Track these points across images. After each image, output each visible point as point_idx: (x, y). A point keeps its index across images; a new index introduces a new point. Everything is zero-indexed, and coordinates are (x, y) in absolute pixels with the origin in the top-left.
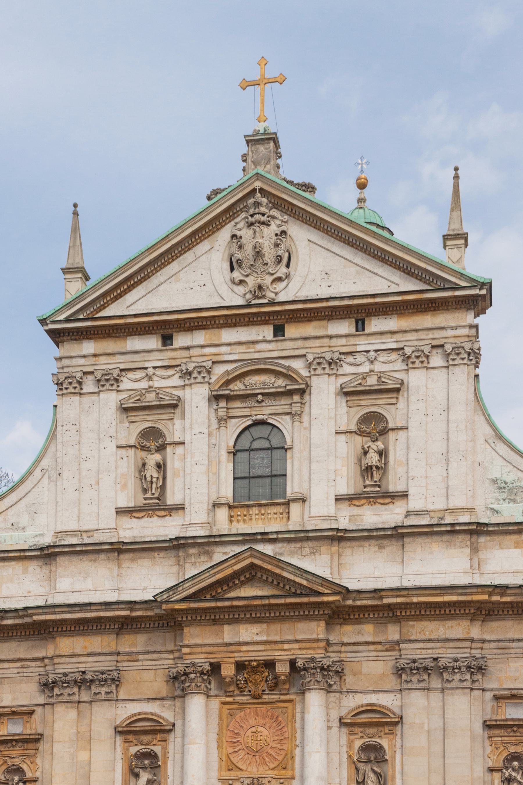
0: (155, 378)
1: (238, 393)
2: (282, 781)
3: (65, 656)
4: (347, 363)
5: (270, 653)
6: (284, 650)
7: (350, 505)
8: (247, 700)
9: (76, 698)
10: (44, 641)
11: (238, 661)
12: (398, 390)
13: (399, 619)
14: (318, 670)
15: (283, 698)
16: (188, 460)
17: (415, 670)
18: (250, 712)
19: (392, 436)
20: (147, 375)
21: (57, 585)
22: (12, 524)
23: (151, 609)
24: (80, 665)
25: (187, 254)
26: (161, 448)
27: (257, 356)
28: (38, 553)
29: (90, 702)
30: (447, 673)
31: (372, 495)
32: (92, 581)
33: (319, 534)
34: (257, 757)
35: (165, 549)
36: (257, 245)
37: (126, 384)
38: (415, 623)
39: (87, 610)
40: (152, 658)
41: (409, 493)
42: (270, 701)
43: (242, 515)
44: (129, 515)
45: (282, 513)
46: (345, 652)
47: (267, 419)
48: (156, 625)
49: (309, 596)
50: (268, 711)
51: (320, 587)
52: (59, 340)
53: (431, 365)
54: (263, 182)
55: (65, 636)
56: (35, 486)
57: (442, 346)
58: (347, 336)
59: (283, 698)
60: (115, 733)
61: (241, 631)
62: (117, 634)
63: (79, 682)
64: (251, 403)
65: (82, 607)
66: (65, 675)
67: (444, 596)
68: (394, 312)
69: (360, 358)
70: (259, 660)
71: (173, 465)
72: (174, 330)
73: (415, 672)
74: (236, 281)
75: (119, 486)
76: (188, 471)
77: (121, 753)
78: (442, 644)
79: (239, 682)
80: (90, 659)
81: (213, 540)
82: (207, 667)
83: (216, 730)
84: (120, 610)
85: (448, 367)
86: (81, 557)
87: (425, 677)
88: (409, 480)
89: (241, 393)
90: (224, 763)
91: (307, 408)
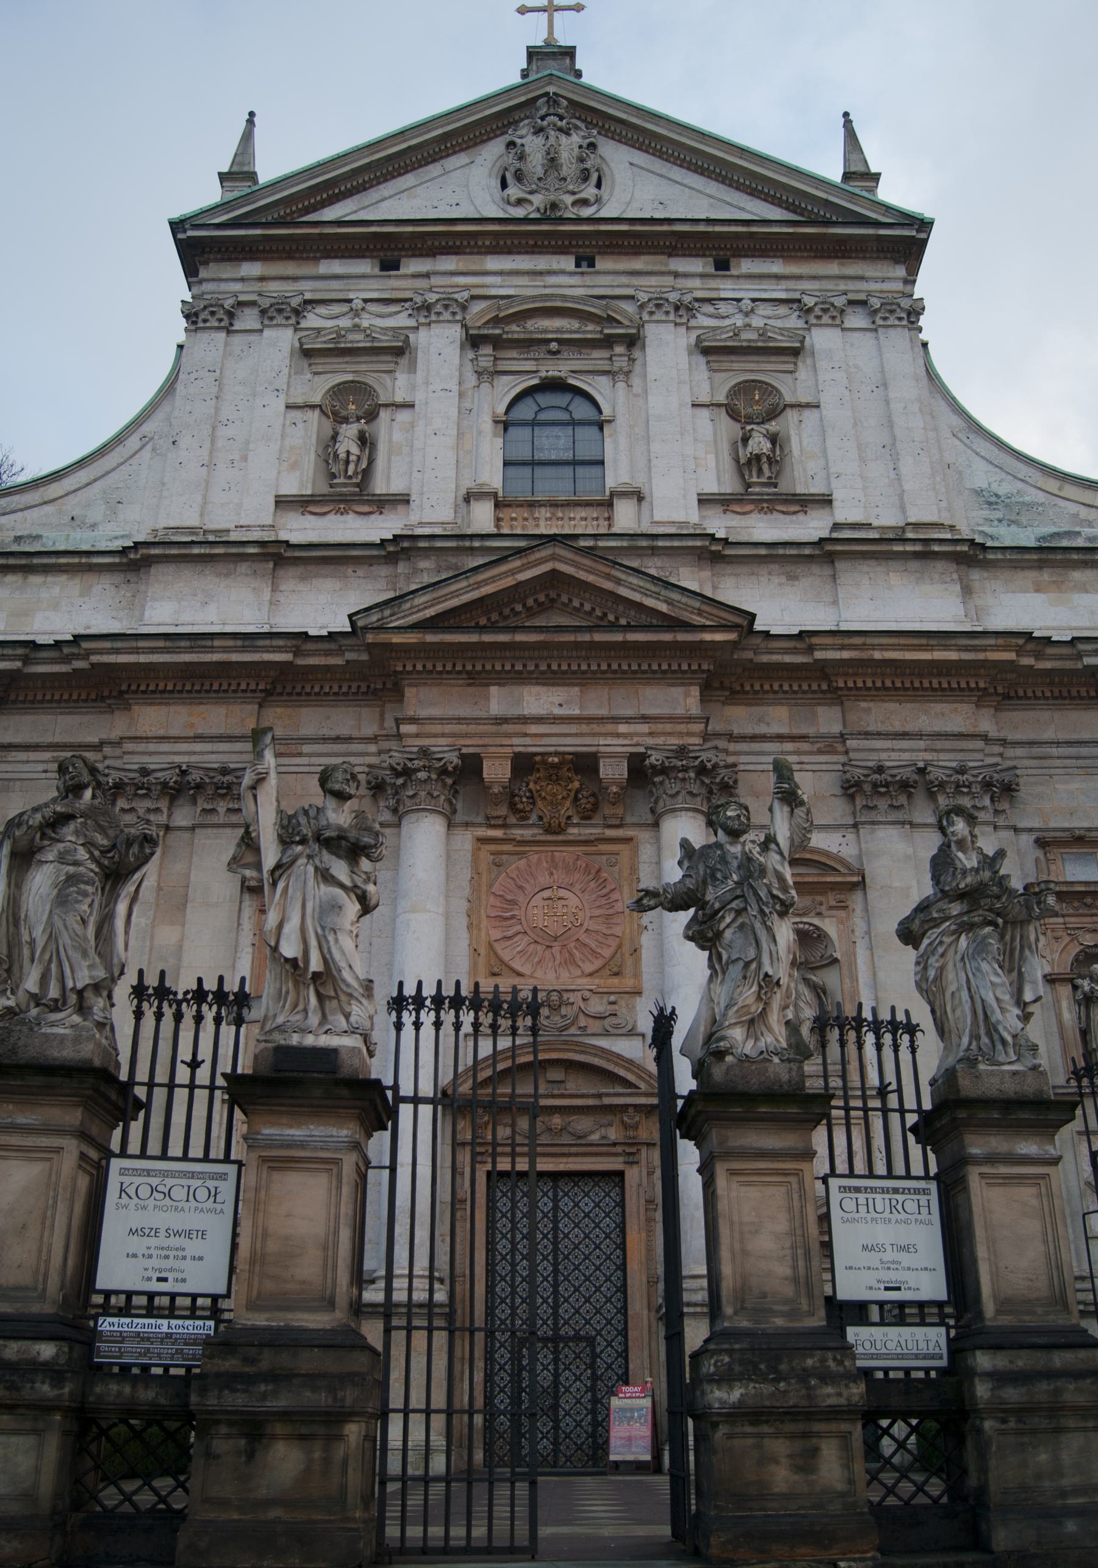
0: (365, 315)
1: (516, 336)
2: (612, 998)
3: (147, 738)
4: (704, 314)
5: (587, 740)
6: (618, 735)
7: (725, 512)
8: (534, 835)
10: (107, 716)
11: (520, 753)
12: (795, 352)
13: (840, 696)
14: (692, 775)
15: (610, 833)
17: (883, 786)
18: (539, 859)
19: (791, 415)
20: (352, 309)
21: (147, 614)
22: (73, 518)
23: (340, 652)
24: (178, 759)
25: (431, 167)
26: (371, 416)
27: (548, 291)
28: (117, 560)
29: (193, 828)
30: (945, 796)
34: (556, 949)
35: (368, 561)
36: (552, 150)
37: (312, 320)
38: (872, 704)
39: (205, 647)
40: (330, 751)
41: (834, 496)
42: (580, 838)
43: (520, 519)
44: (301, 510)
45: (597, 519)
46: (735, 753)
48: (344, 689)
49: (675, 631)
50: (577, 859)
51: (694, 617)
52: (202, 259)
53: (846, 325)
54: (559, 87)
55: (151, 704)
56: (125, 461)
57: (863, 303)
58: (702, 276)
59: (610, 833)
60: (242, 892)
62: (260, 706)
63: (172, 788)
64: (539, 352)
65: (195, 639)
66: (144, 772)
67: (932, 650)
69: (724, 308)
70: (564, 753)
71: (391, 435)
73: (883, 790)
74: (513, 199)
75: (285, 464)
76: (418, 444)
77: (251, 933)
78: (929, 742)
79: (517, 799)
80: (198, 747)
81: (467, 544)
82: (453, 758)
83: (467, 891)
84: (274, 652)
85: (876, 330)
86: (199, 568)
87: (903, 800)
88: (832, 478)
89: (522, 336)
90: (481, 960)
91: (637, 367)
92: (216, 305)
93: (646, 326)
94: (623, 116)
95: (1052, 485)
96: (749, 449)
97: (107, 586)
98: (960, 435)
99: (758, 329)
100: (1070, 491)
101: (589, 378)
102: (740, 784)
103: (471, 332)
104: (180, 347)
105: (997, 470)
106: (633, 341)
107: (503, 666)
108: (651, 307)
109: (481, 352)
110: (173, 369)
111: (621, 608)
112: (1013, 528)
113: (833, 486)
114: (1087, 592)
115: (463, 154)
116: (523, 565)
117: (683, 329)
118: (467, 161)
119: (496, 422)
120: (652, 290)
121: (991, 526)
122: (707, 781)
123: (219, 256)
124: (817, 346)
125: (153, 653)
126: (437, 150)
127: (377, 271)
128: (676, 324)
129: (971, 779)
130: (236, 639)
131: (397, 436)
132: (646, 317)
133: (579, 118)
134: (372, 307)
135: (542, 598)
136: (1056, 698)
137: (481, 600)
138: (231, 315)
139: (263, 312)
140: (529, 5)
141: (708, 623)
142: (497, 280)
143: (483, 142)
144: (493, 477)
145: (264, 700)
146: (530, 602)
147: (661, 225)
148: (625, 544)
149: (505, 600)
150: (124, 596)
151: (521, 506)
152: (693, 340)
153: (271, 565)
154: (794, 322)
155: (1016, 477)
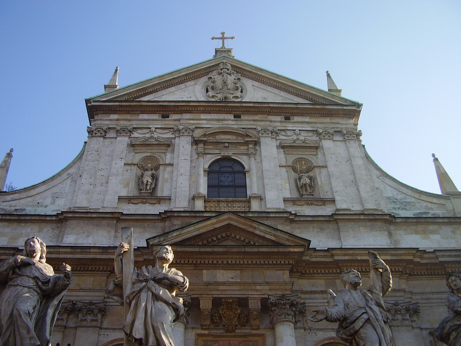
0: (155, 133)
6: (256, 290)
7: (294, 205)
8: (222, 333)
9: (64, 323)
11: (216, 298)
14: (288, 307)
16: (175, 174)
19: (317, 170)
21: (64, 240)
22: (38, 203)
24: (72, 298)
25: (181, 85)
26: (157, 168)
31: (309, 199)
32: (93, 238)
33: (277, 215)
37: (135, 135)
39: (87, 252)
44: (128, 202)
46: (304, 299)
47: (231, 156)
51: (286, 242)
53: (334, 139)
57: (340, 132)
61: (218, 275)
62: (108, 277)
63: (68, 310)
68: (308, 115)
69: (289, 133)
72: (170, 112)
74: (211, 96)
76: (174, 179)
79: (214, 318)
85: (345, 141)
86: (87, 222)
91: (258, 153)
92: (100, 128)
93: (261, 138)
94: (250, 70)
95: (417, 195)
96: (302, 182)
97: (49, 229)
98: (380, 178)
99: (302, 140)
100: (423, 197)
101: (240, 156)
102: (307, 312)
103: (195, 139)
104: (86, 143)
105: (395, 190)
106: (257, 143)
107: (209, 262)
108: (262, 132)
109: (199, 146)
110: (82, 150)
111: (256, 239)
112: (404, 211)
113: (335, 195)
114: (436, 234)
115: (192, 81)
116: (217, 222)
117: (275, 140)
118: (194, 83)
119: (204, 171)
120: (263, 126)
121: (396, 210)
122: (294, 309)
123: (102, 112)
124: (324, 147)
125: (65, 254)
126: (183, 79)
127: (160, 118)
128: (272, 138)
129: (401, 308)
130: (99, 249)
131: (166, 176)
132: (261, 135)
133: (234, 70)
134: (158, 130)
135: (224, 235)
136: (429, 275)
137: (200, 235)
138: (106, 132)
139: (117, 131)
140: (216, 37)
141: (291, 245)
142: (205, 122)
143: (200, 77)
144: (203, 190)
145: (109, 275)
146: (219, 237)
147: (265, 104)
148: (256, 215)
149: (209, 236)
150: (55, 233)
151: (215, 202)
152: (278, 142)
153: (115, 222)
154: (315, 138)
155: (403, 193)
